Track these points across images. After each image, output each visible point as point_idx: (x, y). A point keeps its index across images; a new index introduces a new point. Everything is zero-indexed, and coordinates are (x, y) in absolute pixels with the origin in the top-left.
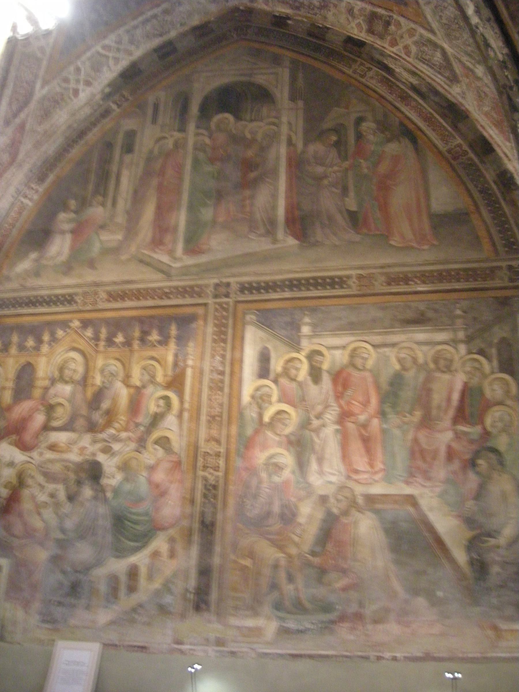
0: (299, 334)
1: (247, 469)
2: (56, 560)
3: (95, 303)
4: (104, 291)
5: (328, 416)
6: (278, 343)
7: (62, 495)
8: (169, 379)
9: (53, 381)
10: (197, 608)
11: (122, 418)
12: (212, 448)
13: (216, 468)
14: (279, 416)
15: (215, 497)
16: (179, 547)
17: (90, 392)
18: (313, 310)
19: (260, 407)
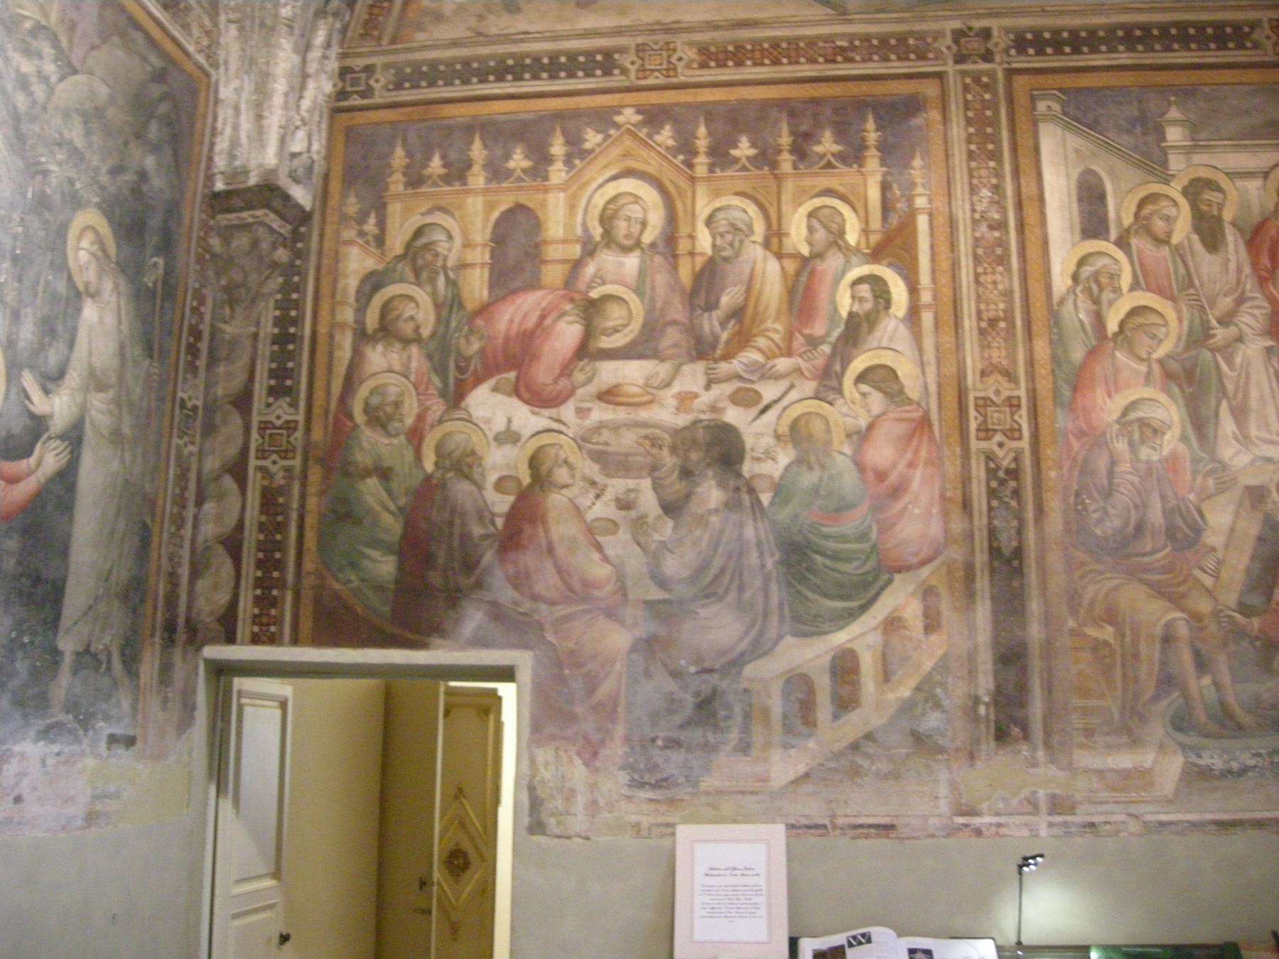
0: (1164, 144)
1: (1081, 434)
2: (649, 646)
3: (671, 69)
4: (691, 44)
5: (1246, 319)
6: (1119, 164)
7: (648, 502)
8: (875, 239)
9: (590, 249)
10: (1001, 736)
11: (775, 328)
12: (996, 387)
13: (1013, 433)
14: (1139, 320)
15: (1016, 493)
16: (945, 606)
17: (685, 272)
18: (1187, 93)
19: (1096, 301)
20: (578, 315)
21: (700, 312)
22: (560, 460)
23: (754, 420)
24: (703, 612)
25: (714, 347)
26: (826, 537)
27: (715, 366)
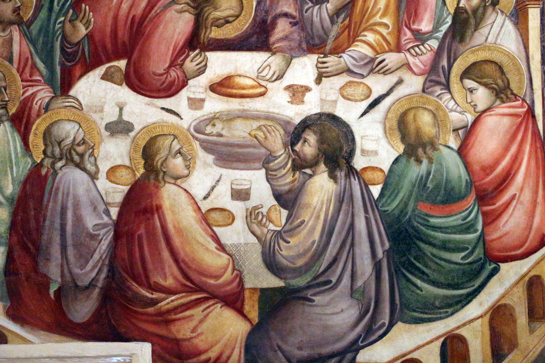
20: (188, 4)
21: (310, 4)
22: (174, 151)
23: (362, 115)
24: (317, 299)
25: (323, 43)
26: (435, 228)
27: (324, 60)
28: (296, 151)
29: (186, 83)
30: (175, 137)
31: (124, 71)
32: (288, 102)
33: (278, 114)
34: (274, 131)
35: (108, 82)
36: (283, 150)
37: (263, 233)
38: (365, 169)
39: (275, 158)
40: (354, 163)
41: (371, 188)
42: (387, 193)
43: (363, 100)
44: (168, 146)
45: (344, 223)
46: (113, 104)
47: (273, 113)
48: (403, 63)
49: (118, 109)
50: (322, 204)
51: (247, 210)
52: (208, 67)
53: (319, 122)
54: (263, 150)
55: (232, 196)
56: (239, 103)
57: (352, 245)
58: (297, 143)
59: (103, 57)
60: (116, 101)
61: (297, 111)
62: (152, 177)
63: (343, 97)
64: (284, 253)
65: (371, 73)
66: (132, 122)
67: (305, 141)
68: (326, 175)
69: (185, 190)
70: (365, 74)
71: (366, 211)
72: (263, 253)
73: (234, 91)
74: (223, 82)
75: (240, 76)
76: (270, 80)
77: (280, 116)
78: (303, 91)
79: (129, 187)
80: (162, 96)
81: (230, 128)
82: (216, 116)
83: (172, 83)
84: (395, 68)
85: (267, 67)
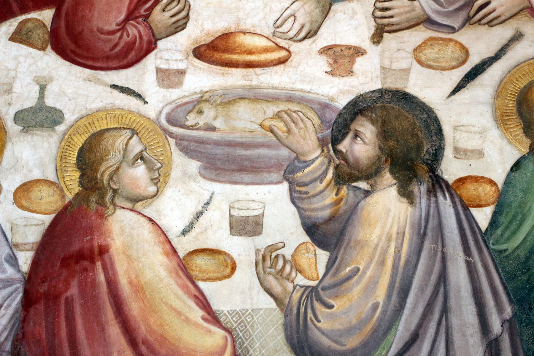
22: (132, 155)
23: (455, 91)
28: (341, 152)
29: (154, 46)
30: (135, 132)
31: (49, 27)
32: (326, 72)
33: (308, 92)
34: (302, 120)
35: (21, 45)
36: (319, 152)
37: (285, 289)
38: (462, 181)
39: (305, 164)
40: (443, 170)
41: (474, 211)
42: (504, 220)
43: (453, 68)
44: (121, 146)
45: (429, 272)
46: (29, 80)
47: (302, 91)
48: (522, 6)
49: (37, 88)
50: (389, 240)
51: (257, 251)
52: (190, 20)
53: (379, 104)
54: (284, 152)
55: (231, 228)
56: (243, 76)
57: (445, 311)
58: (343, 139)
59: (15, 6)
60: (34, 75)
61: (341, 86)
62: (93, 199)
63: (420, 62)
64: (324, 325)
65: (467, 24)
66: (61, 109)
67: (356, 135)
68: (393, 191)
69: (151, 220)
70: (456, 26)
71: (467, 251)
72: (286, 327)
73: (235, 57)
74: (218, 42)
75: (244, 33)
76: (295, 39)
77: (312, 95)
78: (352, 55)
79: (54, 215)
80: (114, 66)
81: (228, 117)
82: (204, 98)
83: (130, 46)
84: (508, 15)
85: (289, 17)
